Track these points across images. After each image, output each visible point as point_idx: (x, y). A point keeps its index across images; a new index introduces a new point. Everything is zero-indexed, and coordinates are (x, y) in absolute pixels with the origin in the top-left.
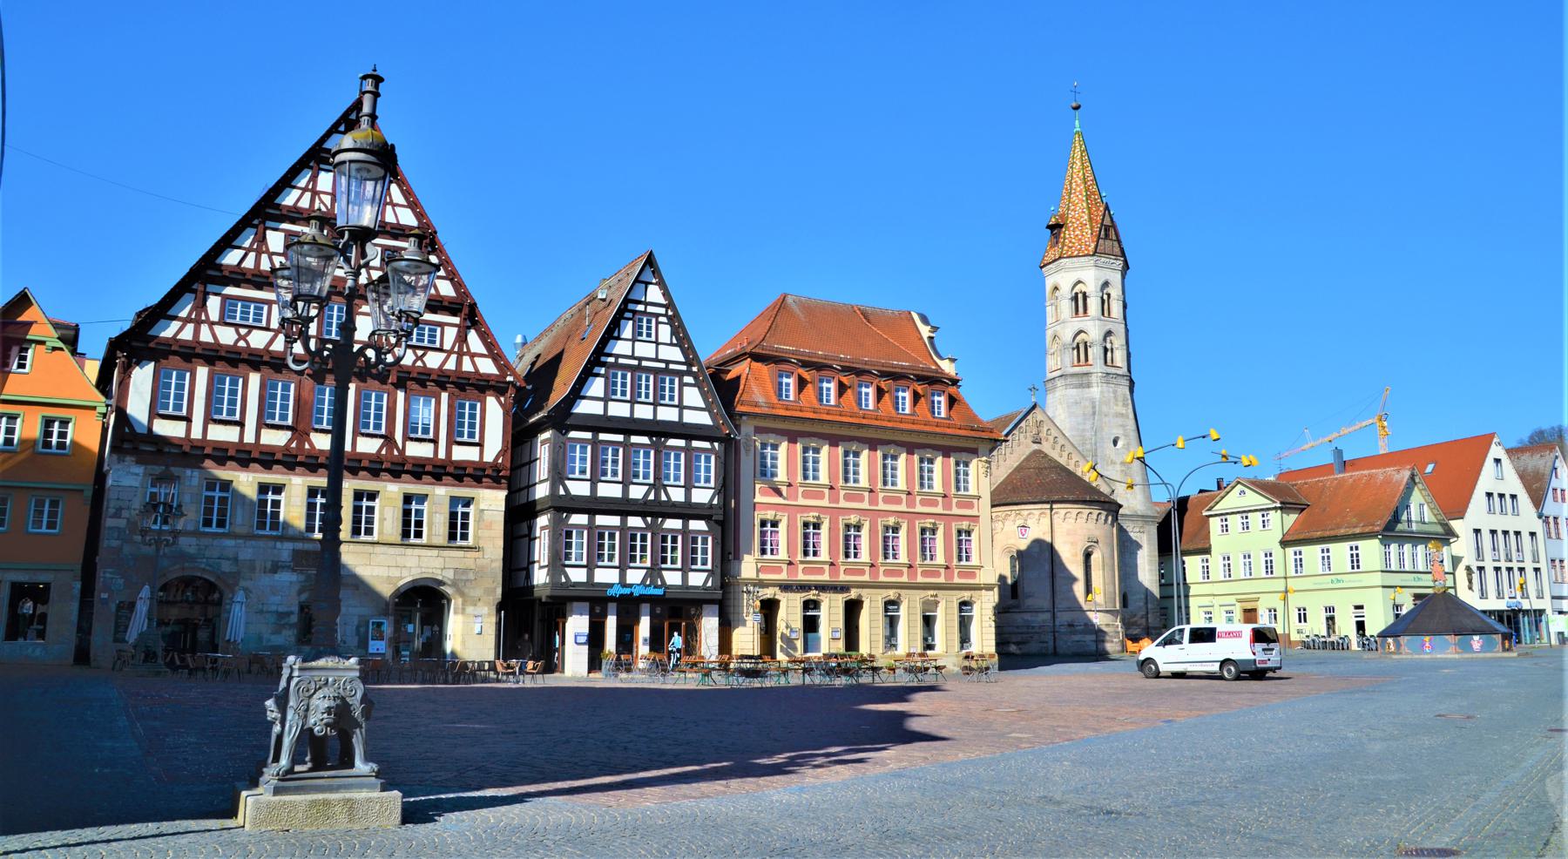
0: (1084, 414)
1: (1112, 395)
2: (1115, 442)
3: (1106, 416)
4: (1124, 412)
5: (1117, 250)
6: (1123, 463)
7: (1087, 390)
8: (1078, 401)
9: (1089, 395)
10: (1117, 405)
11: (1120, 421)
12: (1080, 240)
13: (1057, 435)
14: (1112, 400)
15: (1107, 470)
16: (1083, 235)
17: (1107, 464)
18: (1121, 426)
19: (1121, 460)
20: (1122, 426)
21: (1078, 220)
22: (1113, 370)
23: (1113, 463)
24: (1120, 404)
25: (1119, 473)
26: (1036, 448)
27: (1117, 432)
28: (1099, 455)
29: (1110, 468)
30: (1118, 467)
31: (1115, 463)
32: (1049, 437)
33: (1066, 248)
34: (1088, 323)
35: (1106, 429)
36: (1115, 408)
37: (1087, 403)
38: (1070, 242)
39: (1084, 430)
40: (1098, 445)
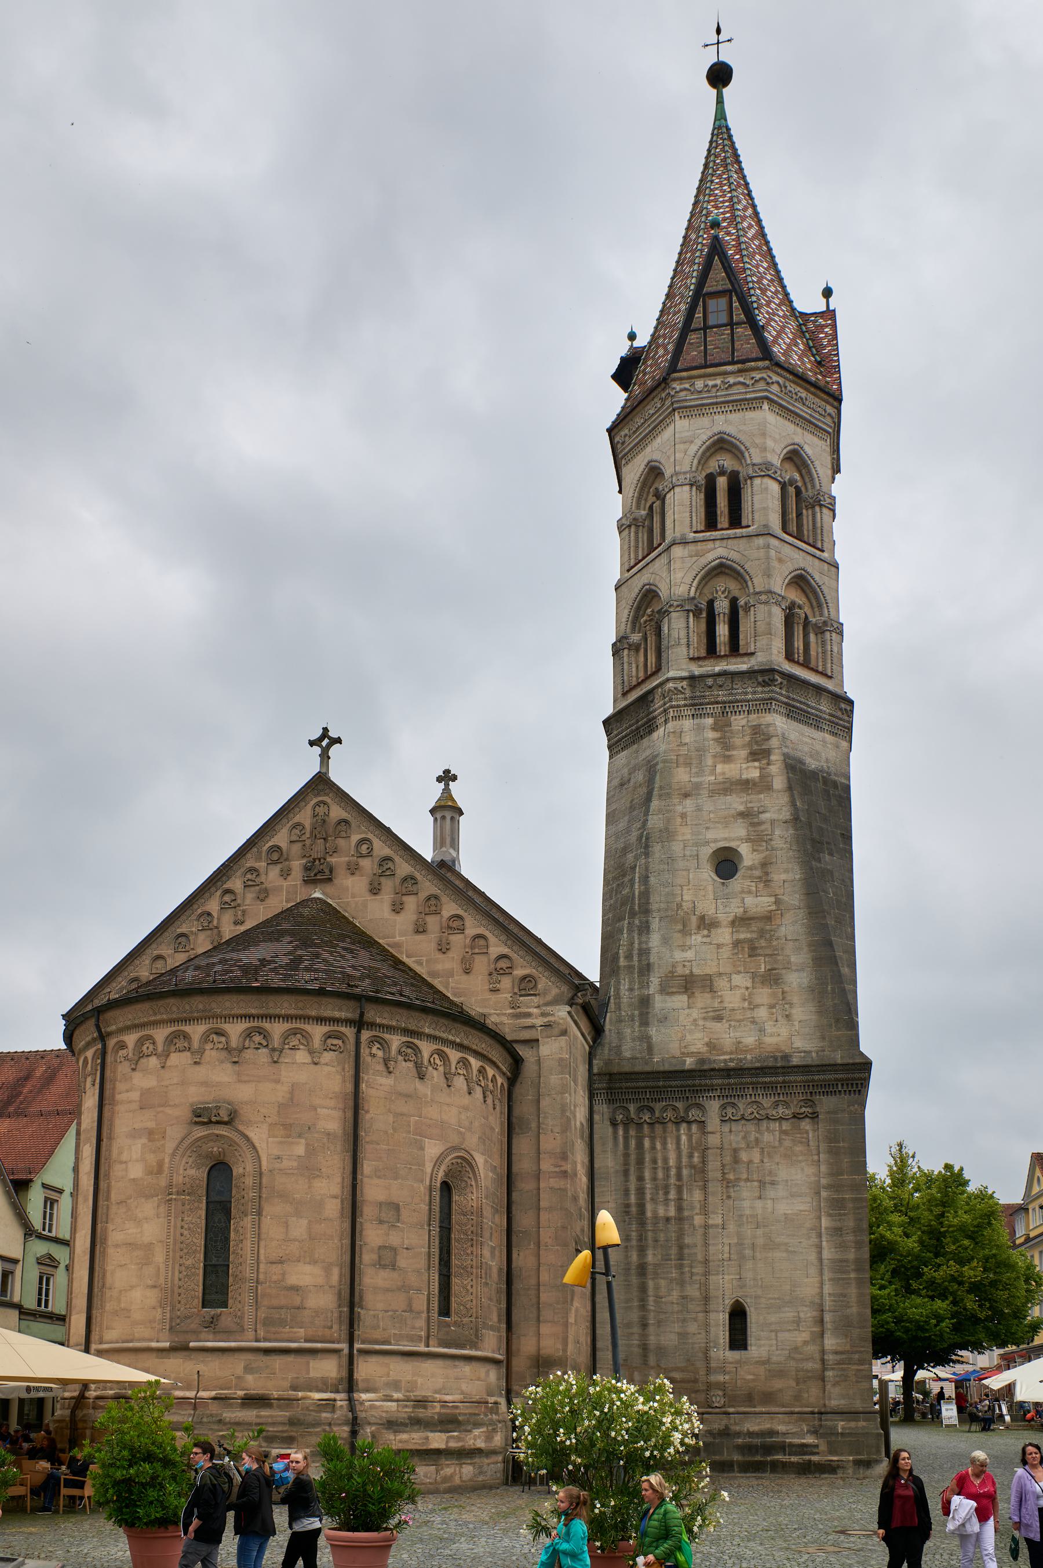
1: (711, 735)
3: (686, 795)
4: (755, 774)
6: (741, 921)
10: (727, 759)
11: (737, 802)
14: (714, 748)
15: (684, 948)
17: (685, 932)
19: (735, 909)
23: (707, 924)
25: (726, 952)
26: (317, 895)
28: (654, 906)
29: (696, 939)
32: (366, 863)
35: (685, 833)
36: (720, 768)
40: (652, 880)
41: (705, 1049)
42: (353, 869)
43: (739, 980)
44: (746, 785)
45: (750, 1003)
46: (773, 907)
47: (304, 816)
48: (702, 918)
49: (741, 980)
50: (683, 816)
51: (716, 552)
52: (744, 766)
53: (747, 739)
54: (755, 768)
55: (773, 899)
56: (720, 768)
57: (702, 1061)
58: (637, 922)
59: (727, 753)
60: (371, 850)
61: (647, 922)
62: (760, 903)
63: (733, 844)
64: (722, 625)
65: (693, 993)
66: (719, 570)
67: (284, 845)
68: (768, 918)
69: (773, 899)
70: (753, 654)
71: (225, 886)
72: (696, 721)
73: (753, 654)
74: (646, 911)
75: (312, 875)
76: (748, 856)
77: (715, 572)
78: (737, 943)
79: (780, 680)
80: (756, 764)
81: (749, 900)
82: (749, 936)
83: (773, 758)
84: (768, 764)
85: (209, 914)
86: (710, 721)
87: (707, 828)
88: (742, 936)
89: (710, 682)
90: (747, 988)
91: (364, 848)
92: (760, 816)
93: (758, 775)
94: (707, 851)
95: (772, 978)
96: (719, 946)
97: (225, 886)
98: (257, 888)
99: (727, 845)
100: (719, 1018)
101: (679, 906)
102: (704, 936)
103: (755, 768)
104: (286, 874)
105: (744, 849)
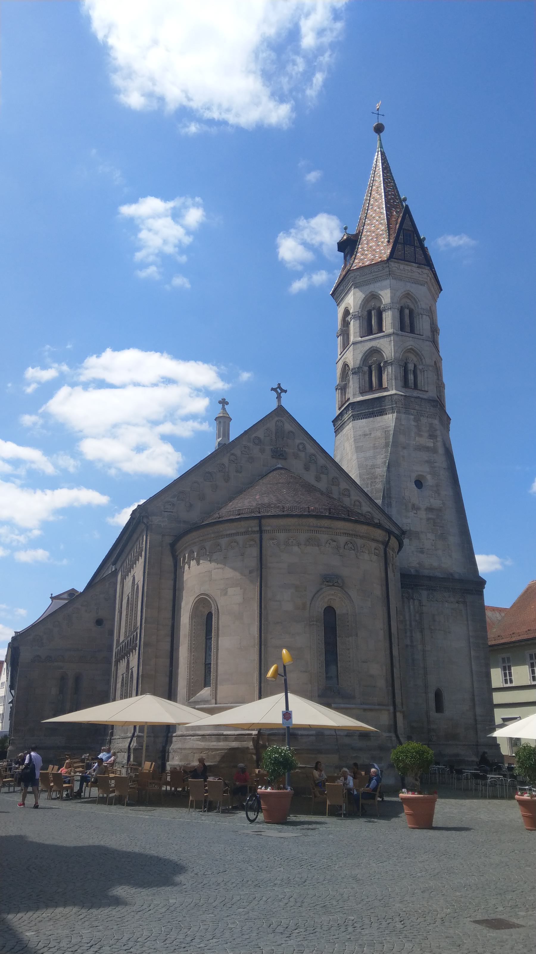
0: (375, 447)
1: (413, 423)
2: (419, 484)
3: (404, 448)
5: (421, 257)
6: (430, 509)
7: (379, 418)
8: (368, 432)
9: (379, 425)
10: (421, 436)
12: (374, 250)
13: (313, 451)
16: (378, 245)
18: (428, 462)
20: (428, 462)
21: (374, 232)
22: (415, 394)
23: (415, 508)
24: (426, 435)
27: (423, 470)
29: (411, 514)
30: (423, 514)
31: (418, 509)
32: (302, 454)
33: (356, 261)
34: (381, 341)
37: (379, 434)
38: (362, 255)
39: (373, 467)
41: (418, 566)
42: (296, 456)
43: (430, 536)
44: (427, 449)
45: (435, 548)
46: (442, 506)
47: (272, 425)
48: (413, 505)
49: (430, 536)
50: (403, 457)
51: (410, 342)
52: (427, 440)
53: (428, 428)
54: (431, 442)
55: (441, 502)
56: (417, 438)
57: (417, 571)
58: (386, 502)
59: (420, 433)
60: (304, 447)
61: (390, 502)
62: (436, 503)
63: (424, 474)
64: (411, 375)
65: (411, 539)
66: (409, 350)
67: (262, 436)
68: (440, 510)
69: (441, 502)
70: (427, 391)
71: (232, 452)
72: (407, 416)
73: (427, 391)
74: (390, 497)
75: (278, 455)
76: (430, 480)
77: (408, 351)
78: (428, 519)
79: (439, 406)
80: (432, 441)
81: (432, 500)
82: (433, 517)
83: (438, 439)
84: (437, 442)
85: (223, 464)
86: (412, 417)
87: (414, 465)
88: (430, 516)
89: (413, 400)
90: (433, 540)
91: (301, 447)
92: (435, 464)
93: (433, 445)
94: (414, 476)
95: (443, 537)
96: (421, 519)
97: (232, 452)
98: (248, 456)
99: (422, 474)
100: (422, 552)
101: (404, 498)
102: (415, 513)
103: (431, 442)
104: (262, 451)
105: (429, 477)
